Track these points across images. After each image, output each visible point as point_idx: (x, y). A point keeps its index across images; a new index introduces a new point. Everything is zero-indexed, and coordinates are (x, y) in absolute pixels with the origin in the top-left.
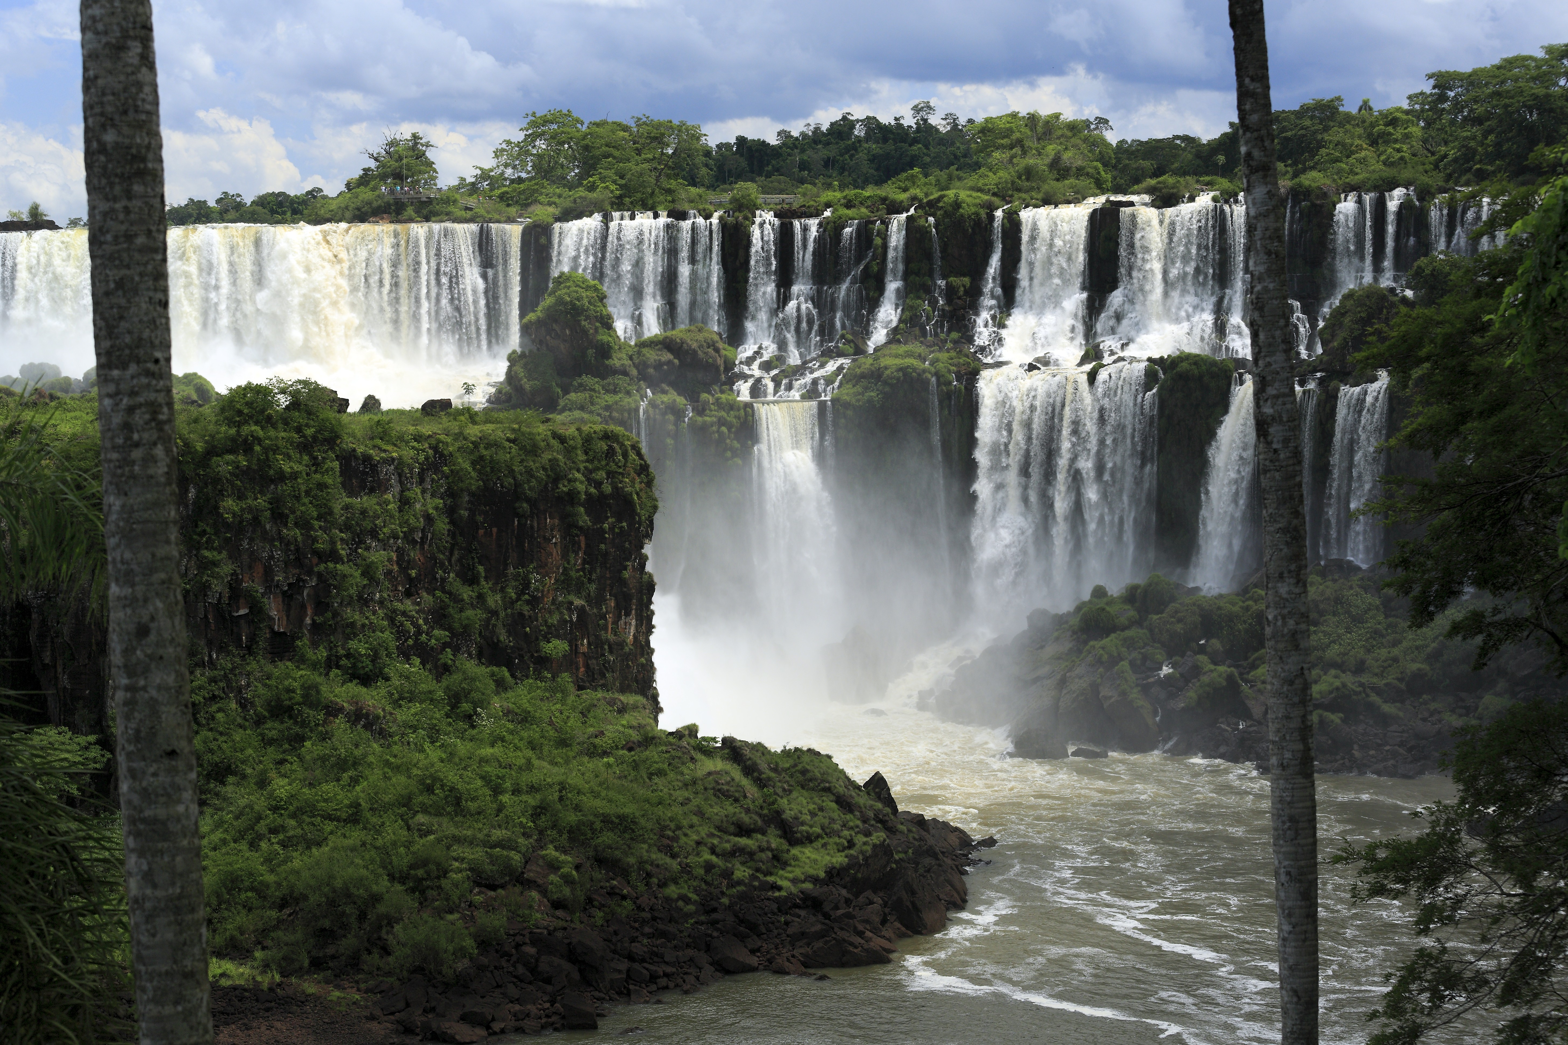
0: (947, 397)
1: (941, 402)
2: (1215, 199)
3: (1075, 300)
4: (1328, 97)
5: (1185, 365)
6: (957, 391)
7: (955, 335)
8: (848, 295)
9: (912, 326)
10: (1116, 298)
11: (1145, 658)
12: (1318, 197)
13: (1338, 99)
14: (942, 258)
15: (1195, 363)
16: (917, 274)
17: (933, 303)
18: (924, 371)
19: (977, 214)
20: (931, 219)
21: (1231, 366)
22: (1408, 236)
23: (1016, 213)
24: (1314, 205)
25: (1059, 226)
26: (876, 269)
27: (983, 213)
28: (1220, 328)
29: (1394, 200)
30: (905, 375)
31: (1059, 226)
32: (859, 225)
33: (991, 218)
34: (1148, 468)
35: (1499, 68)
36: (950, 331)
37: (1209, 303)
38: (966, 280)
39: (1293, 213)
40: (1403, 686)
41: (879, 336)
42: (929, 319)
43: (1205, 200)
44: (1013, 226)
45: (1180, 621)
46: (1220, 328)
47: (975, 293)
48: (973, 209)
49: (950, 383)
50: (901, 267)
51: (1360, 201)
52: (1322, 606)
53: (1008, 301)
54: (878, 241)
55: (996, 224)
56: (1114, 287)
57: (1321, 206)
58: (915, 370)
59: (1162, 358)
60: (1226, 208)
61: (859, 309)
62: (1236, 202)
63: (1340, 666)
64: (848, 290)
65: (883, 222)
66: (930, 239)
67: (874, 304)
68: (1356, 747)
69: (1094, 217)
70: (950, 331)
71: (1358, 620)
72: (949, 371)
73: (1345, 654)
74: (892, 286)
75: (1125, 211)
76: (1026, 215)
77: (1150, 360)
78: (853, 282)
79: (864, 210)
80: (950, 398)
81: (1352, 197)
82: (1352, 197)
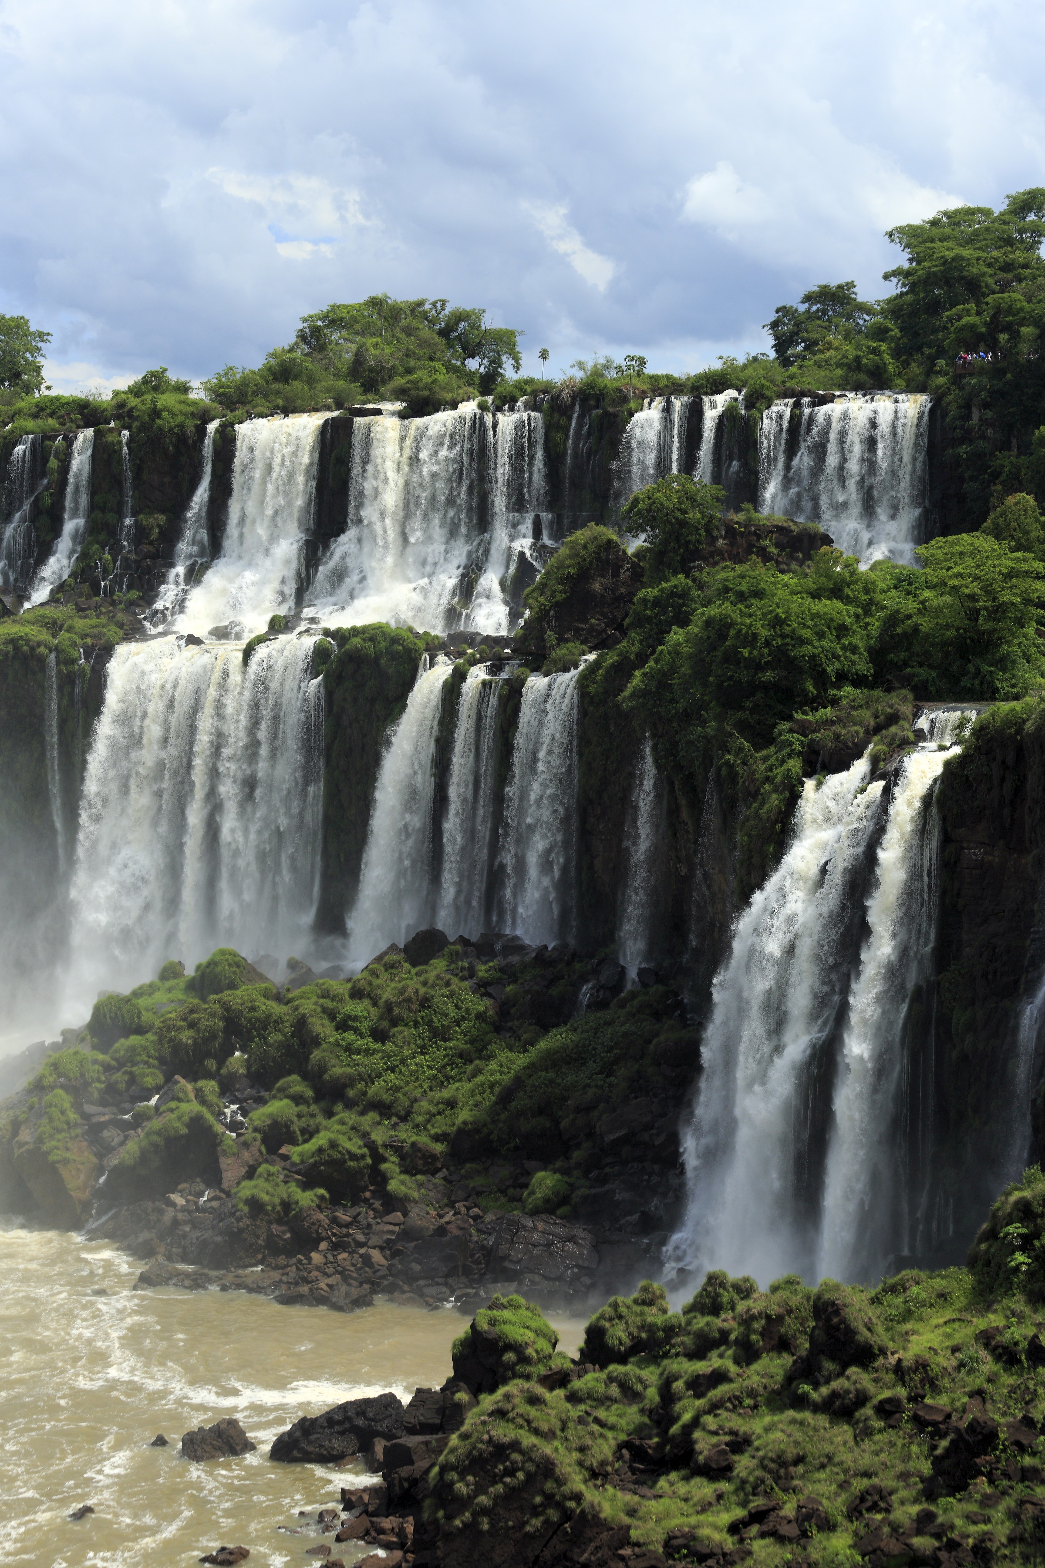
0: (68, 680)
1: (60, 689)
2: (482, 407)
3: (288, 547)
4: (833, 283)
5: (356, 641)
6: (83, 672)
7: (134, 594)
8: (14, 537)
9: (83, 581)
10: (344, 544)
11: (132, 1079)
12: (614, 403)
13: (851, 285)
14: (135, 488)
15: (371, 639)
16: (103, 510)
17: (116, 550)
18: (39, 644)
19: (181, 426)
20: (126, 433)
21: (421, 644)
22: (731, 459)
23: (232, 425)
24: (606, 414)
25: (278, 442)
26: (48, 501)
27: (191, 426)
28: (467, 589)
29: (715, 408)
30: (17, 649)
31: (278, 442)
32: (34, 441)
33: (202, 432)
34: (311, 789)
35: (935, 223)
36: (130, 587)
37: (460, 553)
38: (162, 518)
39: (580, 425)
40: (439, 1148)
41: (40, 594)
42: (105, 571)
43: (468, 408)
44: (227, 443)
45: (192, 1025)
46: (467, 589)
47: (171, 535)
48: (180, 419)
49: (74, 661)
50: (84, 499)
51: (667, 409)
52: (396, 1011)
53: (213, 548)
54: (53, 463)
55: (207, 441)
56: (341, 529)
57: (615, 415)
58: (28, 641)
59: (338, 630)
60: (488, 419)
61: (26, 557)
62: (512, 409)
63: (383, 1109)
64: (15, 529)
65: (65, 438)
66: (120, 461)
67: (44, 551)
68: (323, 1246)
69: (324, 430)
70: (130, 587)
71: (440, 1034)
72: (74, 645)
73: (396, 1089)
74: (71, 525)
75: (359, 421)
76: (244, 429)
77: (327, 633)
78: (23, 520)
79: (51, 422)
80: (72, 683)
81: (659, 402)
82: (659, 402)
